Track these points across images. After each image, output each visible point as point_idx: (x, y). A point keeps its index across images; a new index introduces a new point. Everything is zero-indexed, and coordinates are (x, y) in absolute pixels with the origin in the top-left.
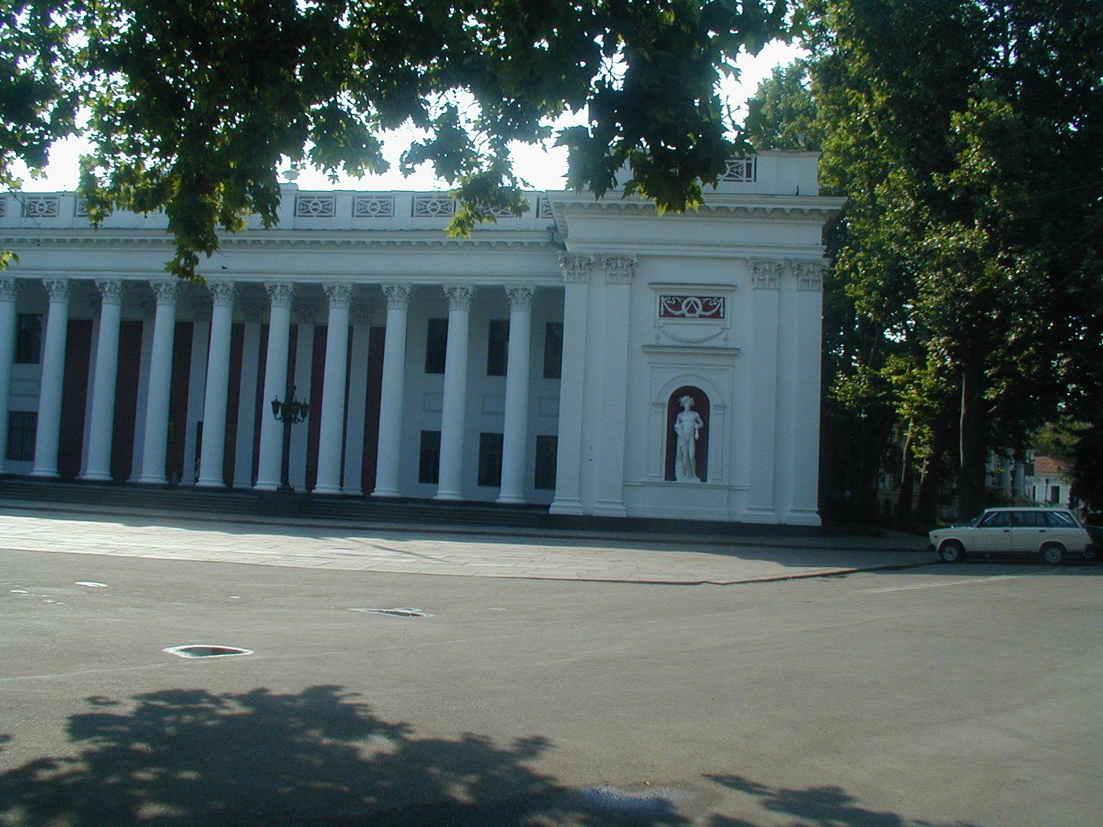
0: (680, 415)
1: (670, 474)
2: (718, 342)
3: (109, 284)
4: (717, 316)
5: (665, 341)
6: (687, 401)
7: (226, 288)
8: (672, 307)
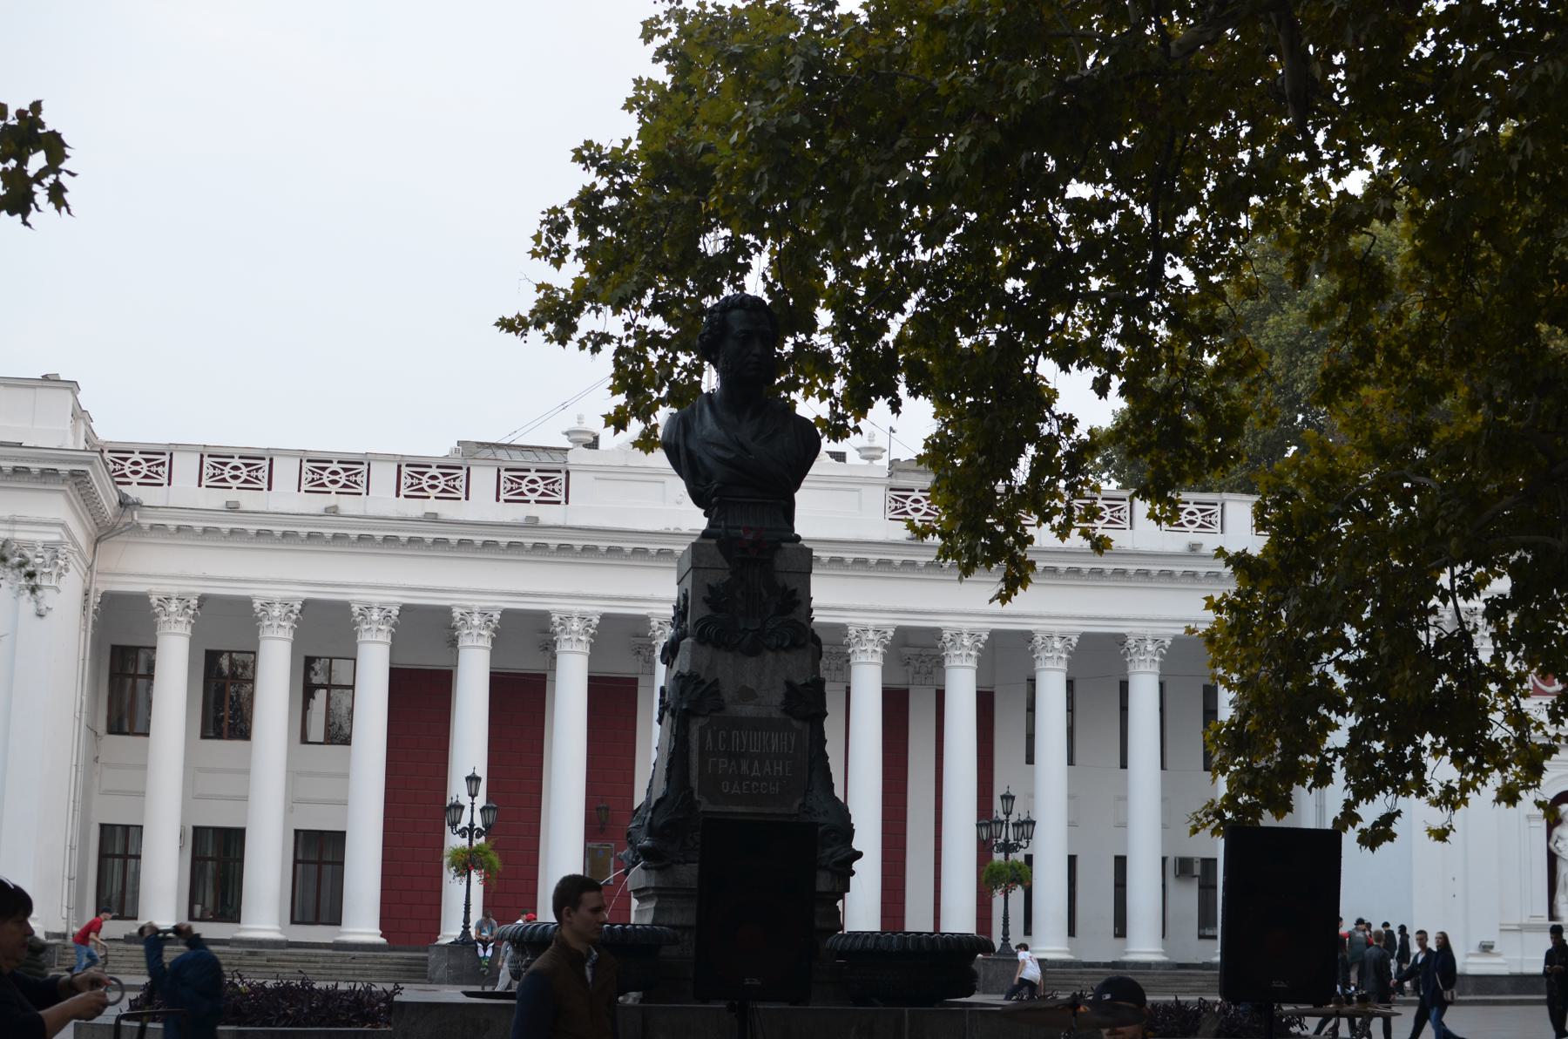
0: (1557, 831)
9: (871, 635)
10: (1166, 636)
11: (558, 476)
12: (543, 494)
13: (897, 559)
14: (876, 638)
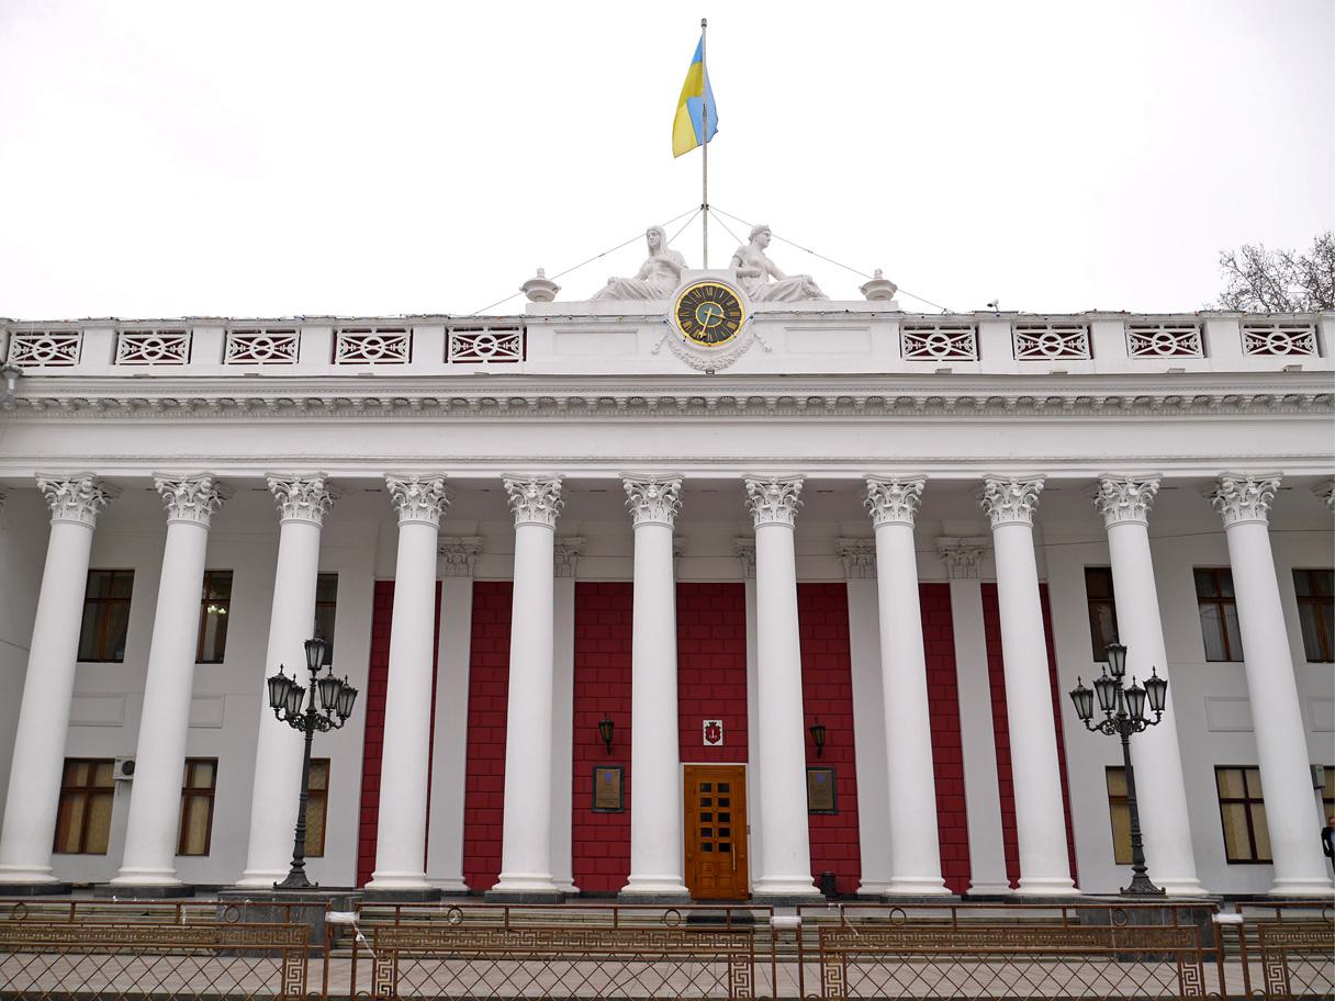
3: (533, 485)
7: (785, 490)
9: (895, 489)
10: (1272, 476)
11: (515, 333)
12: (498, 353)
13: (921, 395)
14: (904, 493)
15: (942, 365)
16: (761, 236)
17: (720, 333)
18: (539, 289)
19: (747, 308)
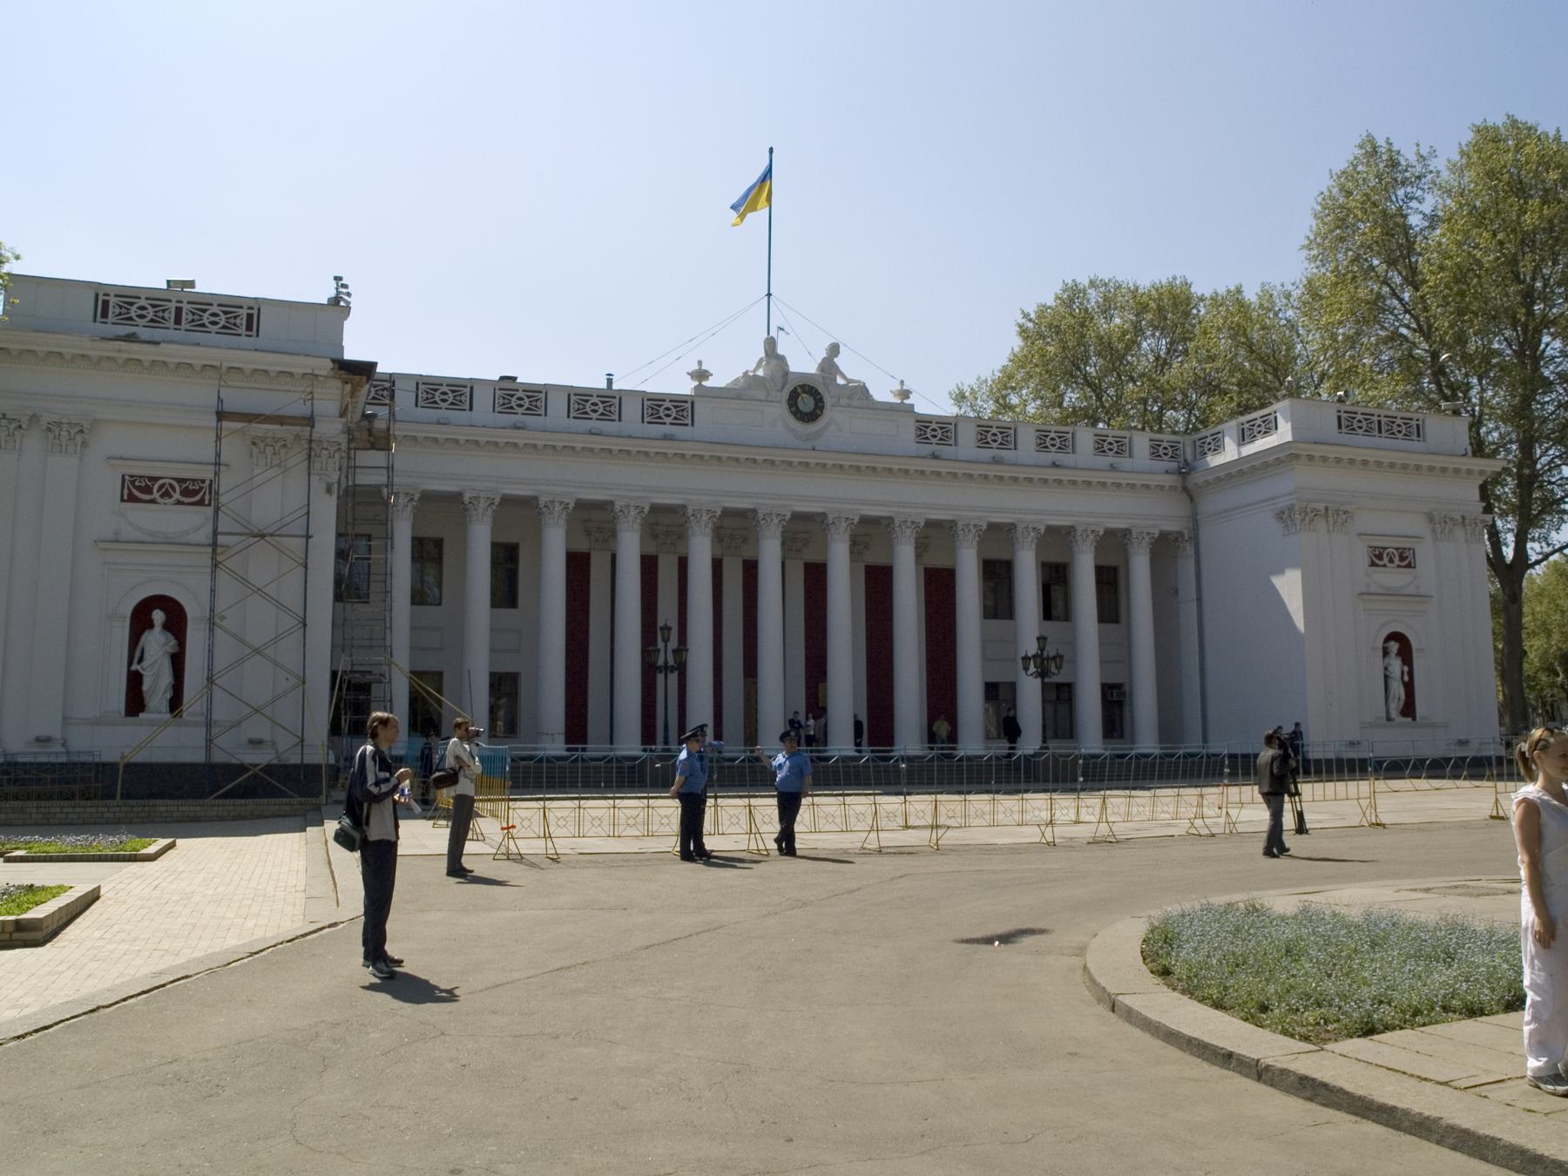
1: (1389, 719)
2: (1411, 590)
4: (1409, 566)
5: (1373, 589)
6: (1394, 646)
8: (1377, 557)
15: (933, 448)
16: (834, 350)
17: (811, 417)
18: (701, 375)
19: (828, 401)
